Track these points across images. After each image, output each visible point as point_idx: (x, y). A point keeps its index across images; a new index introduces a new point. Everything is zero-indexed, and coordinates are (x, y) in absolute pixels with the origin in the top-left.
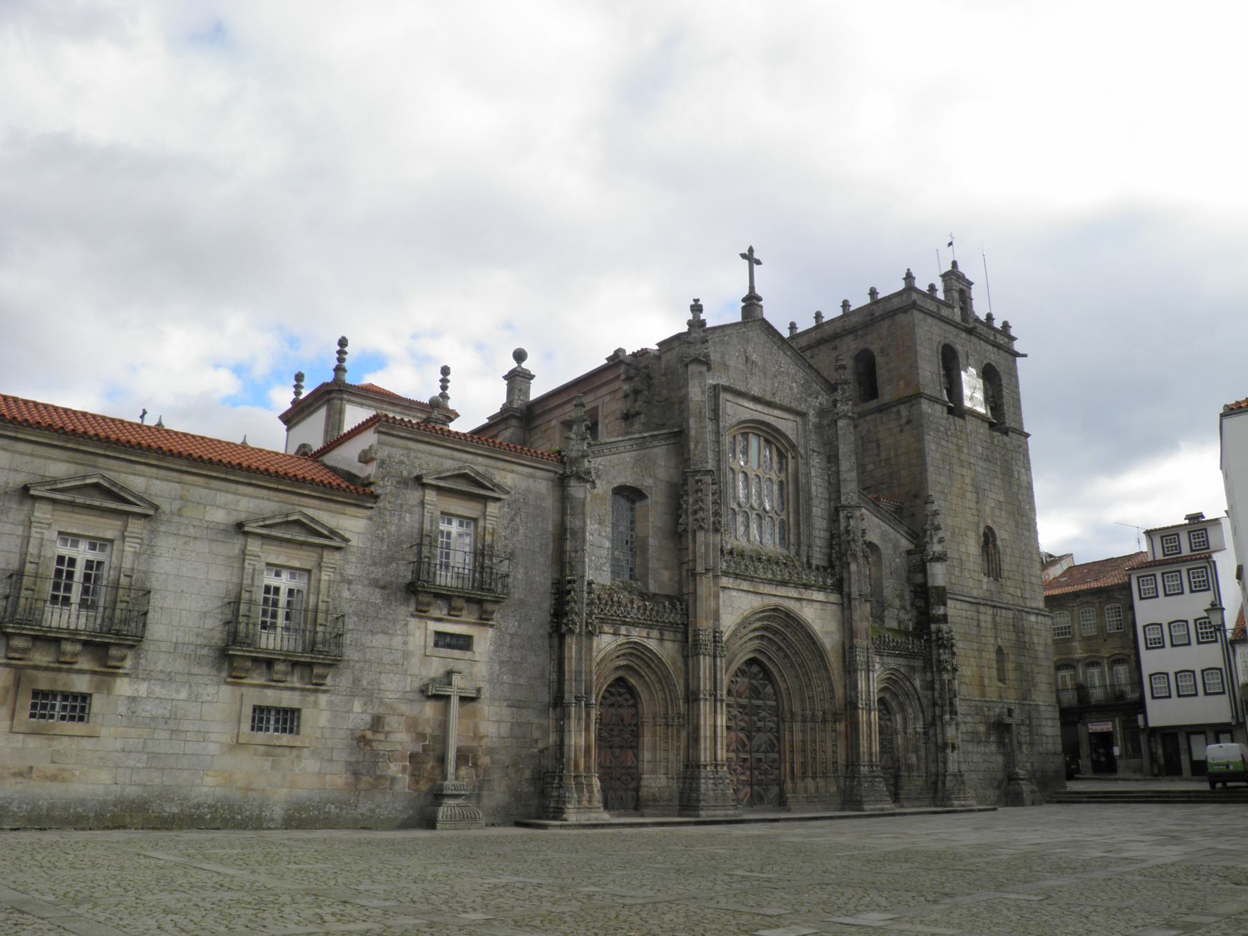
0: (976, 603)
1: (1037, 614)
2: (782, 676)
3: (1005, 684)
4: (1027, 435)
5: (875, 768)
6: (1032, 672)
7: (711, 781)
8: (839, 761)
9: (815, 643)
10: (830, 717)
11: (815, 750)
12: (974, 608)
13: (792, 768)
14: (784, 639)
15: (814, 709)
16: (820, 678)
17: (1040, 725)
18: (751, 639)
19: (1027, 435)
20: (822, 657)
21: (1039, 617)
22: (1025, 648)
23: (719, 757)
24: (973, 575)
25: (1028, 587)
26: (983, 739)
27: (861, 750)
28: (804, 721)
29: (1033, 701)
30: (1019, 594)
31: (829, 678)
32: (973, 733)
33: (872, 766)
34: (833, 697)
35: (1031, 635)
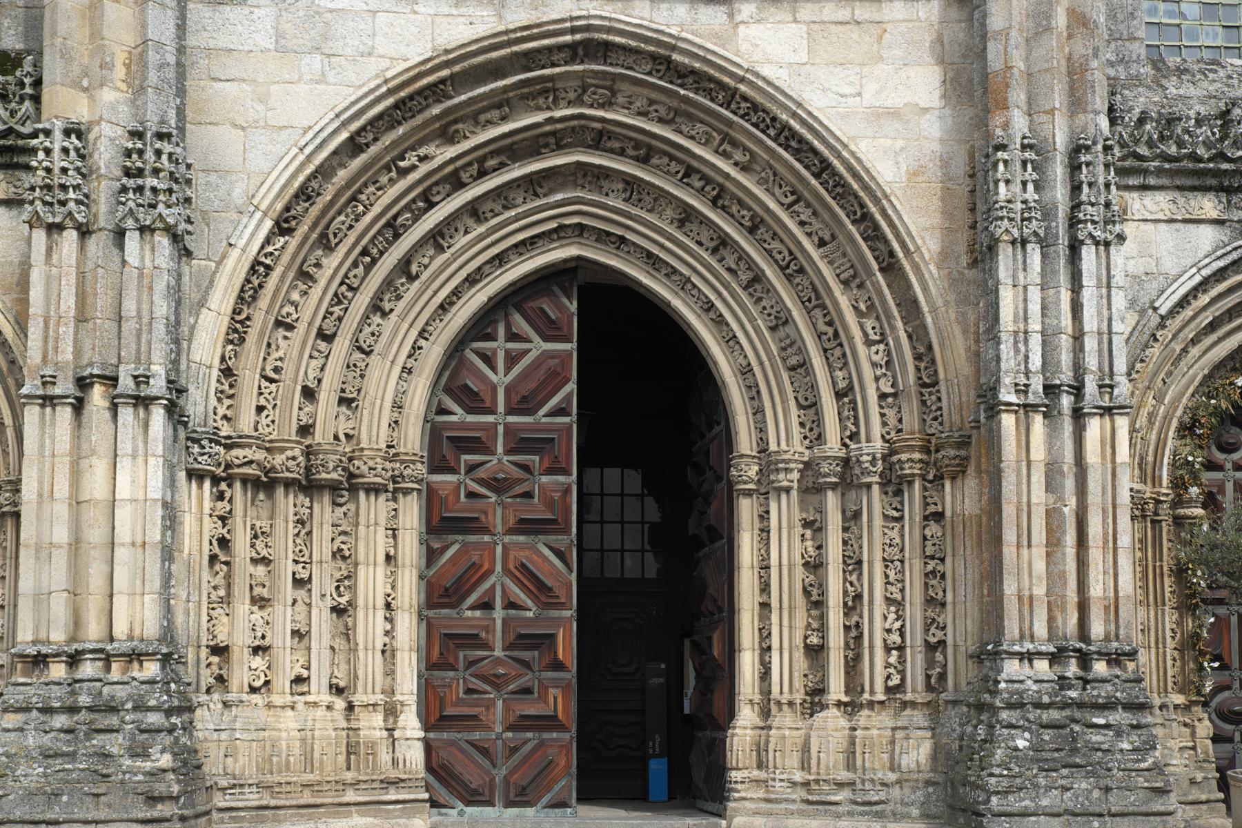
2: (720, 321)
5: (1100, 668)
7: (60, 721)
8: (950, 641)
9: (823, 169)
10: (910, 462)
11: (858, 597)
13: (765, 675)
14: (689, 171)
15: (854, 436)
16: (871, 307)
18: (532, 184)
20: (864, 219)
23: (120, 630)
27: (1010, 588)
28: (812, 489)
31: (910, 307)
33: (1085, 660)
34: (929, 384)
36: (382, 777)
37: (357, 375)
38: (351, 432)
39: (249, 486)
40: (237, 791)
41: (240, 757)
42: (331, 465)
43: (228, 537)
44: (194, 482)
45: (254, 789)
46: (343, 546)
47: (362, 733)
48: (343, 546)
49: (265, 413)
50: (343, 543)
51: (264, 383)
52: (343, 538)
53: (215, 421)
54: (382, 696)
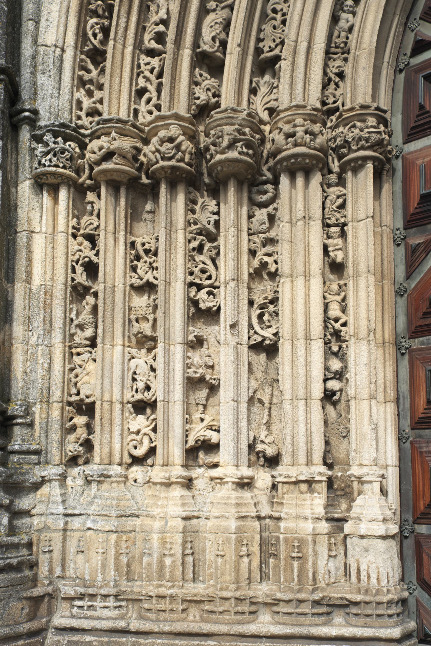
36: (317, 596)
37: (277, 23)
38: (273, 104)
39: (123, 192)
40: (85, 603)
41: (92, 554)
42: (225, 143)
43: (95, 259)
44: (45, 194)
45: (111, 602)
46: (266, 259)
47: (282, 524)
48: (266, 259)
49: (147, 95)
50: (269, 255)
51: (145, 58)
52: (269, 249)
53: (79, 118)
54: (323, 469)
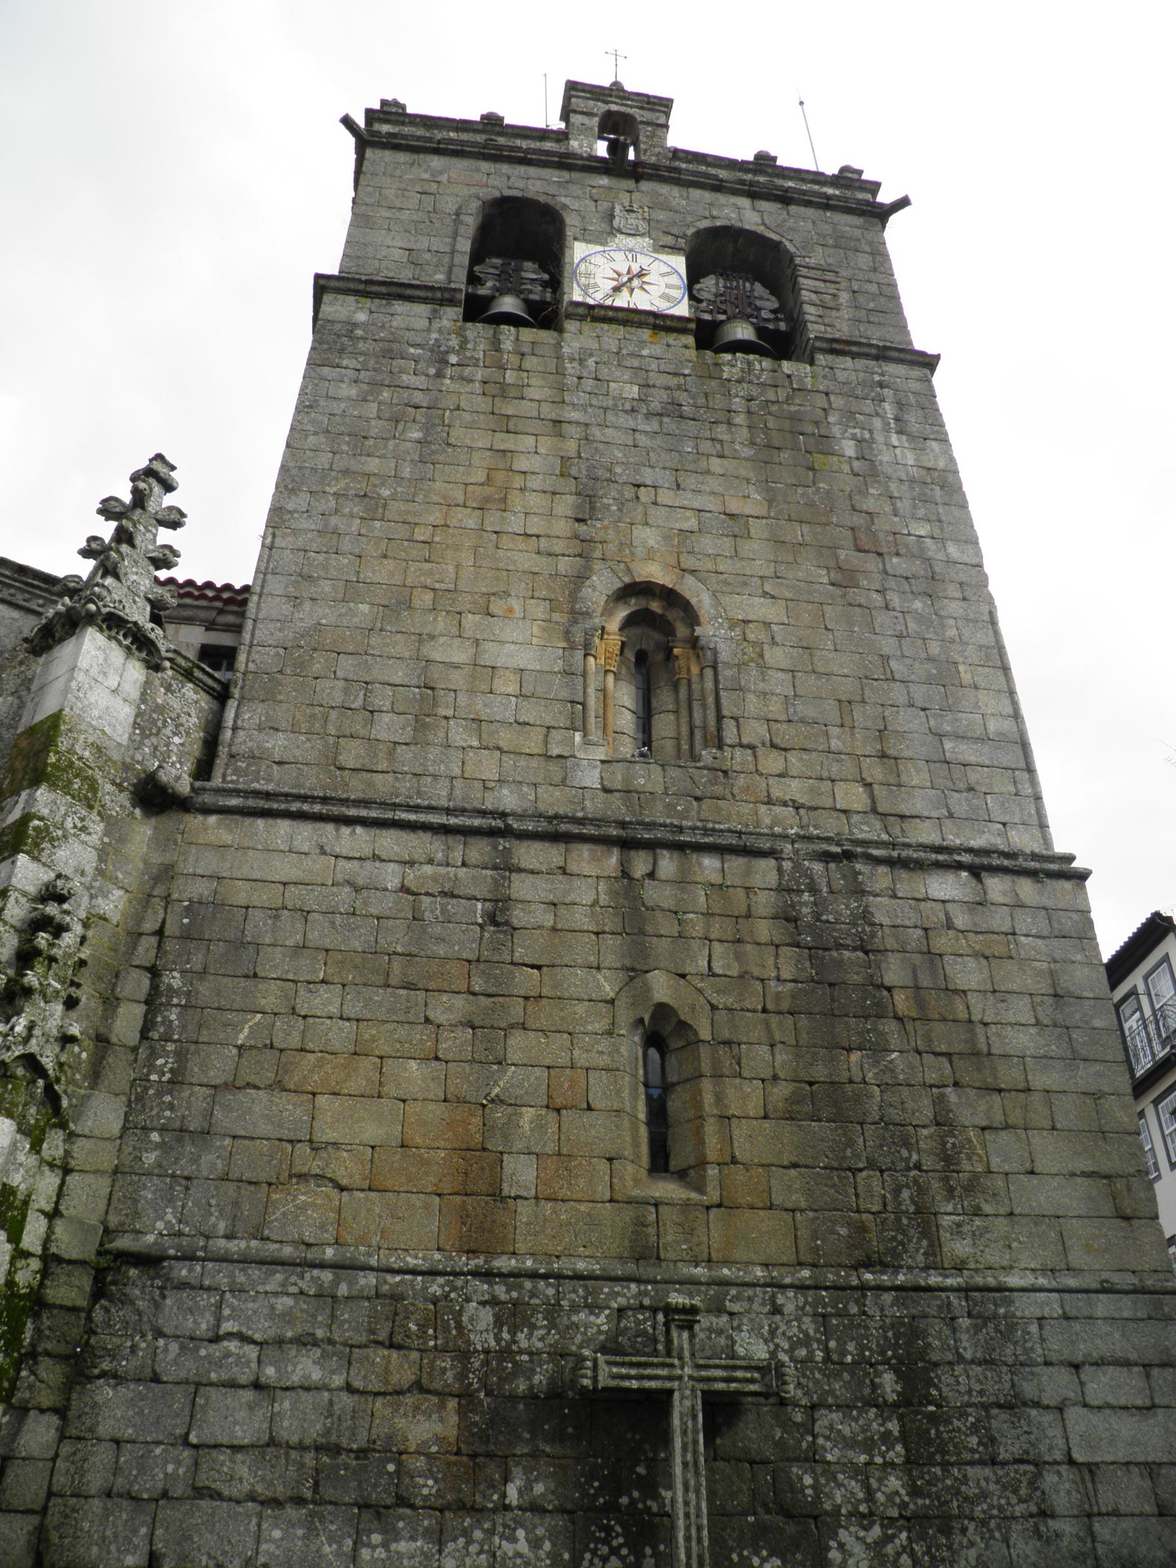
0: (492, 833)
1: (976, 872)
3: (700, 1189)
4: (930, 362)
6: (943, 1121)
12: (479, 850)
17: (1014, 1405)
19: (930, 362)
21: (996, 886)
22: (880, 1012)
24: (505, 738)
25: (916, 776)
26: (428, 1487)
29: (959, 1267)
30: (853, 797)
32: (335, 1450)
35: (932, 957)
